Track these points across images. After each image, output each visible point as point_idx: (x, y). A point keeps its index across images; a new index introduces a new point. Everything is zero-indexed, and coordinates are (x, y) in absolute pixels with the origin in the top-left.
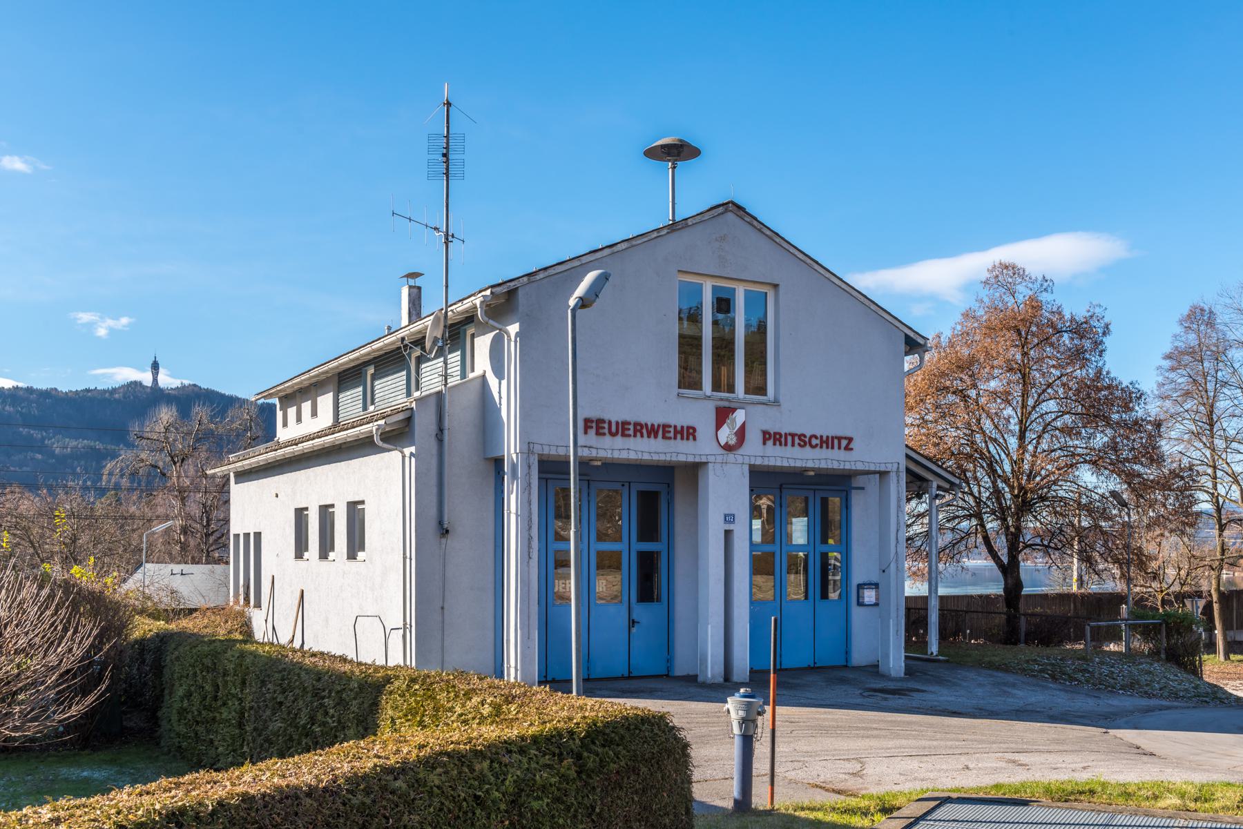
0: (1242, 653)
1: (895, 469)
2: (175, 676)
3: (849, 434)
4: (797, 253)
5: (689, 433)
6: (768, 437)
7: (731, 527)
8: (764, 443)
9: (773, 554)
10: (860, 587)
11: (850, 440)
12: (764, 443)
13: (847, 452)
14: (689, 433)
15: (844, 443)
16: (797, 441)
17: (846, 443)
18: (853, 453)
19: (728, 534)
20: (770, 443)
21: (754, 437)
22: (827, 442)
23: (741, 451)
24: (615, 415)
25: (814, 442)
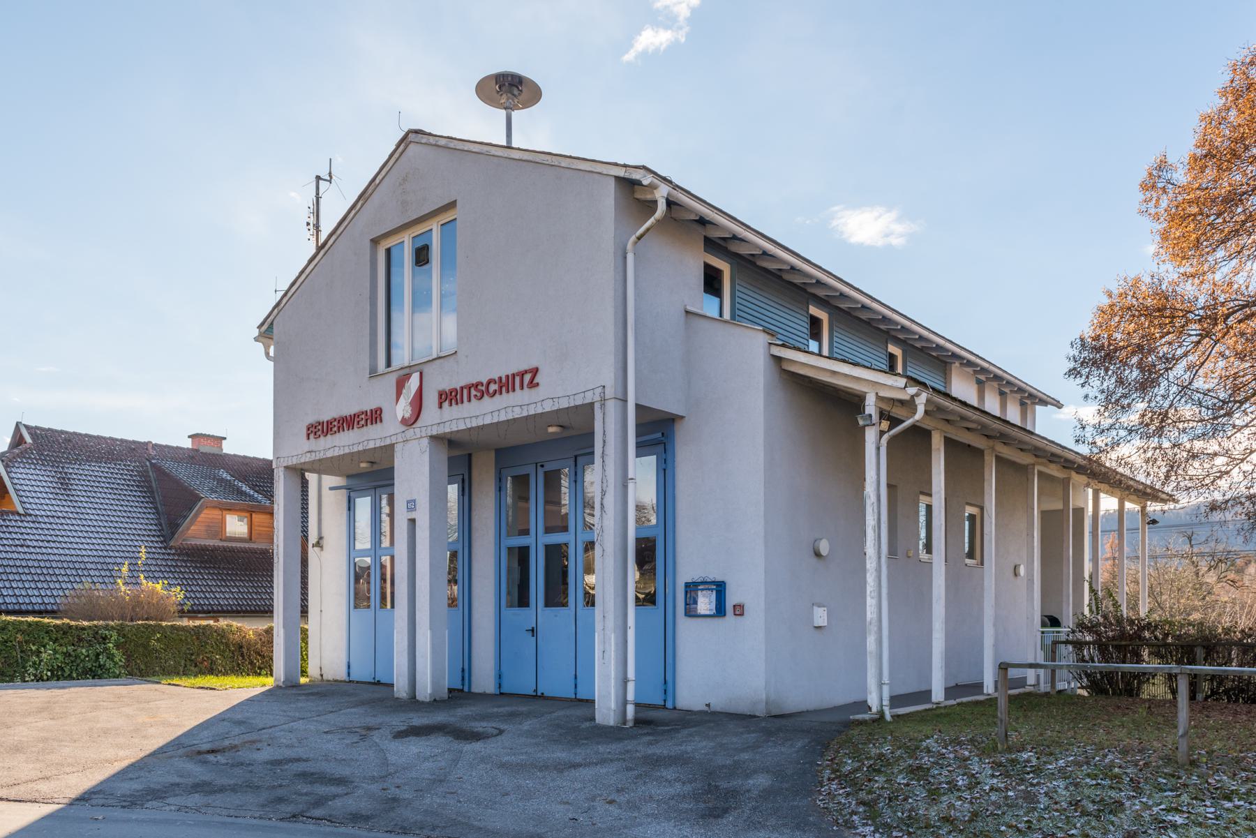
0: (3, 628)
1: (597, 398)
2: (958, 748)
3: (533, 364)
4: (380, 177)
5: (375, 416)
6: (449, 397)
7: (412, 515)
8: (441, 407)
9: (528, 548)
10: (692, 588)
11: (535, 371)
12: (441, 407)
13: (534, 391)
14: (375, 416)
15: (527, 377)
16: (473, 392)
17: (529, 378)
18: (540, 387)
19: (412, 522)
20: (446, 404)
21: (430, 399)
22: (506, 384)
23: (419, 423)
24: (328, 414)
25: (493, 387)
